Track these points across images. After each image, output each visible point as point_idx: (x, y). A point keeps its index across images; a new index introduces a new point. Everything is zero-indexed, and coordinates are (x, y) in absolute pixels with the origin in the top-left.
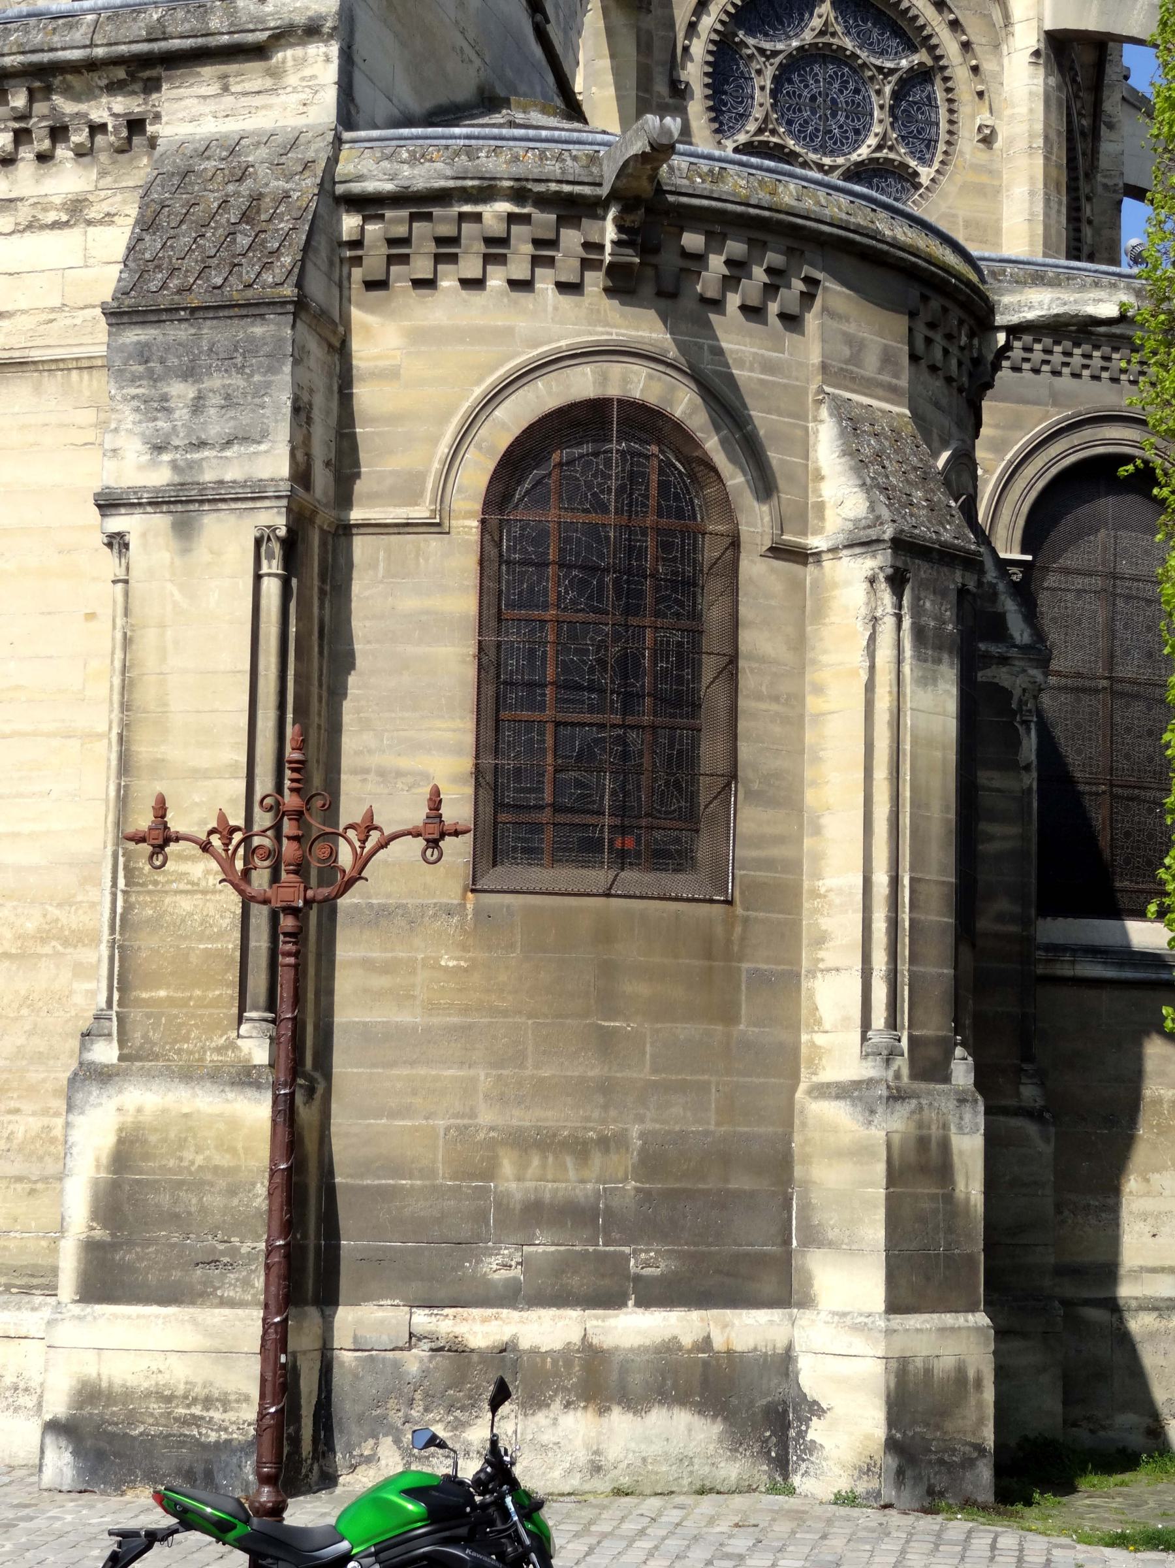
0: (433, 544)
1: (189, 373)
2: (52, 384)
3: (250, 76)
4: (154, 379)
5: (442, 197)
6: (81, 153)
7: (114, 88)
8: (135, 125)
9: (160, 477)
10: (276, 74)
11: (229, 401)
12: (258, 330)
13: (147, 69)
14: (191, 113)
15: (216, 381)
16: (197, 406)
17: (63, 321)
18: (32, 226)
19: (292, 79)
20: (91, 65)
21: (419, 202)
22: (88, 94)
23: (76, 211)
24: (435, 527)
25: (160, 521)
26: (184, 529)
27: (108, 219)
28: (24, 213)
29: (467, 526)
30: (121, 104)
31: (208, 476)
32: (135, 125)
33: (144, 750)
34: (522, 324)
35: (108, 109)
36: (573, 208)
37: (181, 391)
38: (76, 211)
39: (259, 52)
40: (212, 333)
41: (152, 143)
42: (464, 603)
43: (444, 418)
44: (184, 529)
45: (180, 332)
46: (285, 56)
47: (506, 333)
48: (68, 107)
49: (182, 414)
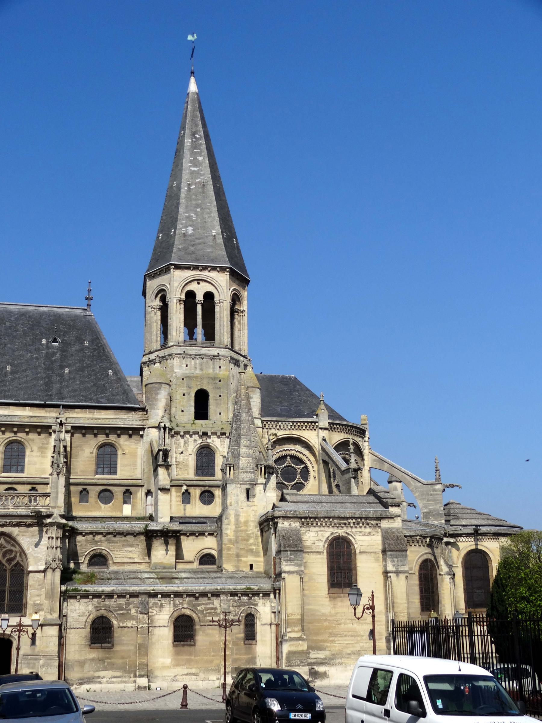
0: (414, 575)
1: (396, 558)
2: (368, 555)
3: (391, 521)
4: (392, 558)
5: (413, 536)
6: (370, 527)
7: (374, 520)
8: (377, 524)
9: (394, 569)
10: (394, 520)
11: (401, 561)
12: (404, 553)
13: (379, 519)
14: (385, 524)
15: (399, 559)
16: (398, 561)
17: (369, 547)
18: (364, 535)
19: (396, 521)
20: (373, 517)
21: (411, 536)
22: (371, 520)
23: (370, 533)
24: (415, 574)
25: (395, 575)
26: (397, 575)
27: (374, 535)
28: (363, 533)
29: (417, 574)
30: (375, 522)
31: (400, 569)
32: (377, 524)
33: (395, 601)
34: (420, 550)
35: (373, 522)
36: (425, 537)
37: (396, 560)
38: (370, 533)
39: (393, 518)
40: (398, 553)
41: (380, 527)
42: (417, 582)
43: (414, 561)
44: (397, 575)
45: (395, 553)
46: (396, 518)
47: (419, 551)
48: (369, 521)
49: (396, 562)
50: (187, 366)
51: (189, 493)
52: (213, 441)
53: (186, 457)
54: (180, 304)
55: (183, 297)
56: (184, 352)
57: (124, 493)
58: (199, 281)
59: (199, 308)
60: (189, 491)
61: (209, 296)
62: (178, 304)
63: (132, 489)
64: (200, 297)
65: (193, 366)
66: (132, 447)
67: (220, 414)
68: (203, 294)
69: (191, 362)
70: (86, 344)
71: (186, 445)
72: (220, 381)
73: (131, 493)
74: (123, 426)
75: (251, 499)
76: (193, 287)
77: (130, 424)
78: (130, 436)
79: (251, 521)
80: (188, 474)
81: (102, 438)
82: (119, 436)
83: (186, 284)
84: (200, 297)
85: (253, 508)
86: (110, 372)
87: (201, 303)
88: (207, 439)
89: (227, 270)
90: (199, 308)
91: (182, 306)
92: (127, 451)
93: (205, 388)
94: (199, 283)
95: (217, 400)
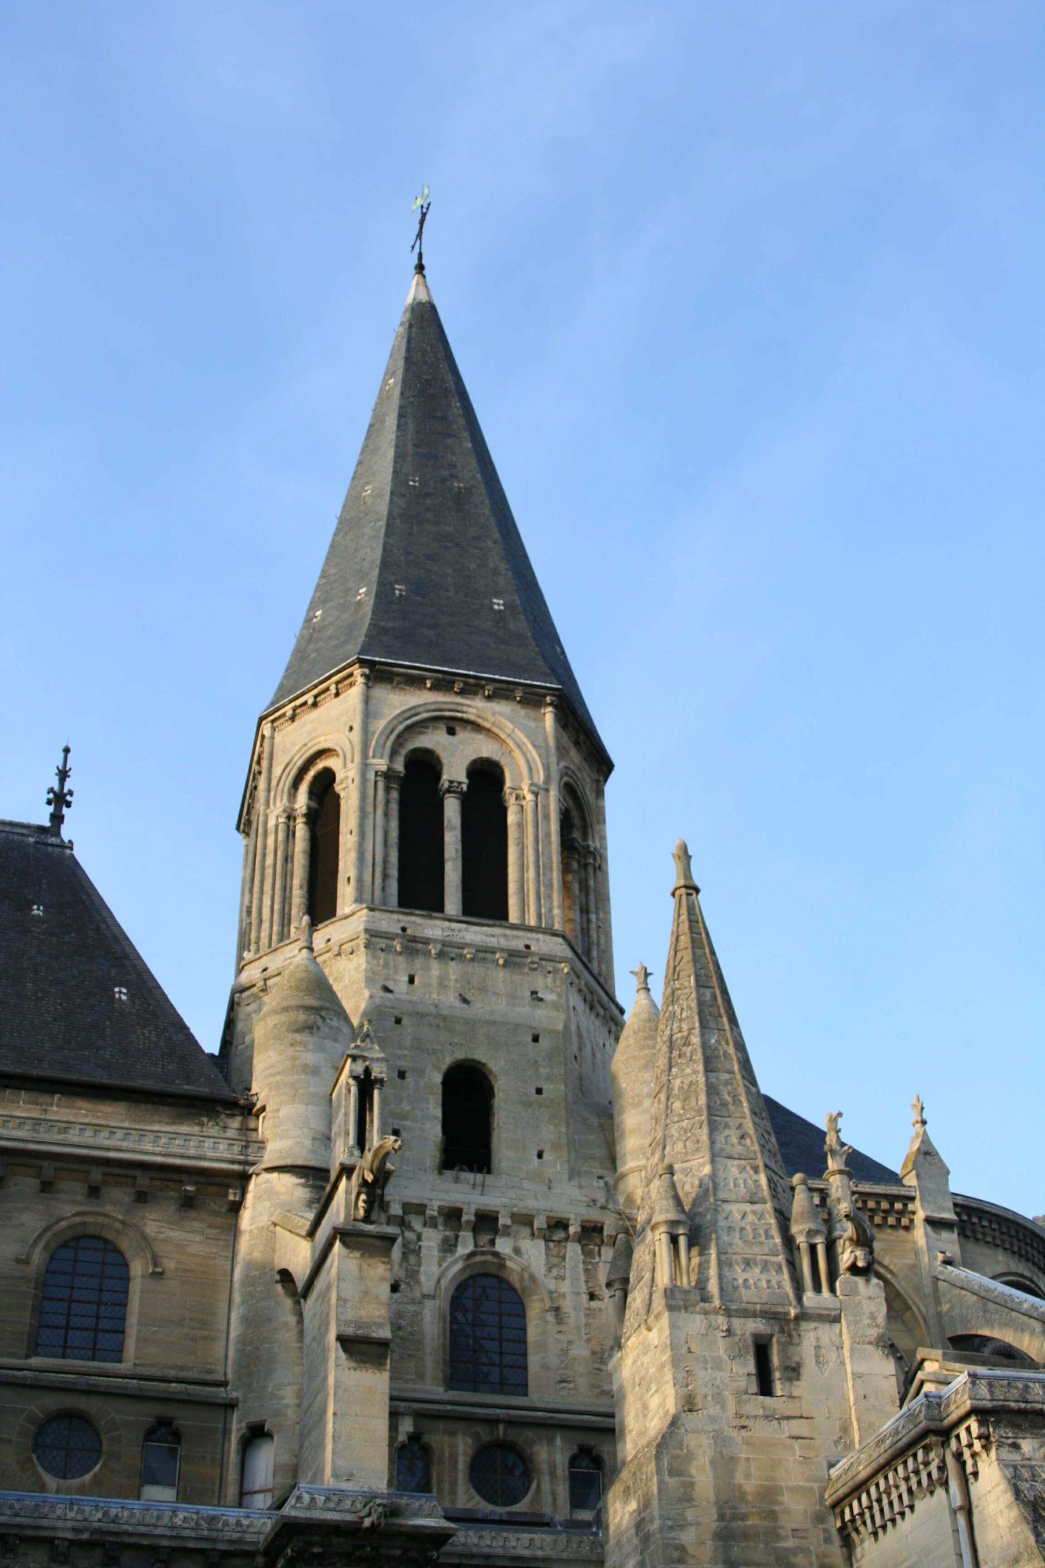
50: (411, 980)
51: (426, 1450)
52: (517, 1251)
53: (411, 1308)
54: (388, 789)
55: (399, 766)
56: (404, 929)
57: (150, 1434)
58: (453, 724)
59: (452, 809)
60: (426, 1438)
61: (487, 777)
62: (381, 785)
63: (185, 1419)
64: (455, 771)
65: (434, 982)
66: (191, 1249)
67: (540, 1155)
68: (466, 763)
69: (427, 969)
70: (37, 911)
71: (412, 1259)
72: (536, 1039)
73: (177, 1436)
74: (159, 1159)
75: (778, 1387)
76: (434, 740)
77: (192, 1152)
78: (188, 1203)
79: (788, 1489)
80: (420, 1376)
81: (69, 1208)
82: (142, 1197)
83: (408, 728)
84: (455, 771)
85: (797, 1427)
86: (121, 993)
87: (461, 793)
88: (492, 1242)
89: (548, 699)
90: (452, 809)
91: (395, 795)
92: (169, 1265)
93: (480, 1055)
94: (451, 732)
95: (530, 1104)
